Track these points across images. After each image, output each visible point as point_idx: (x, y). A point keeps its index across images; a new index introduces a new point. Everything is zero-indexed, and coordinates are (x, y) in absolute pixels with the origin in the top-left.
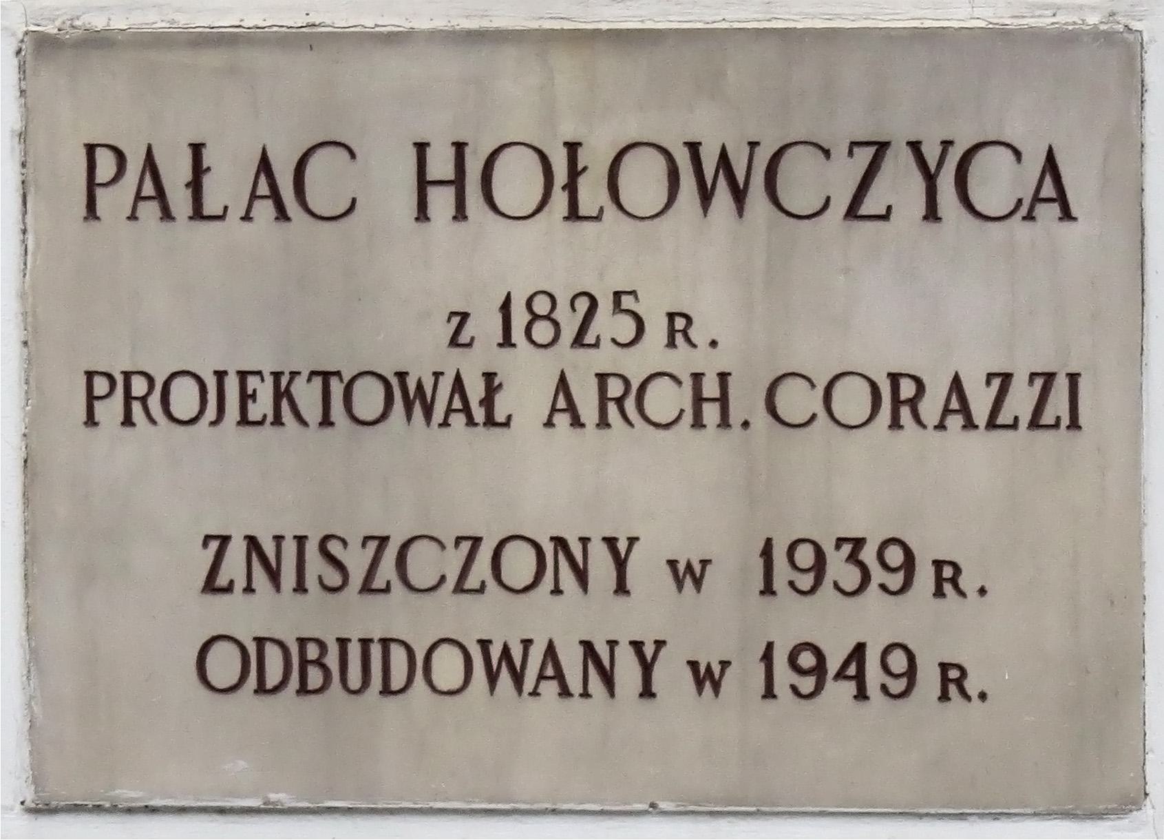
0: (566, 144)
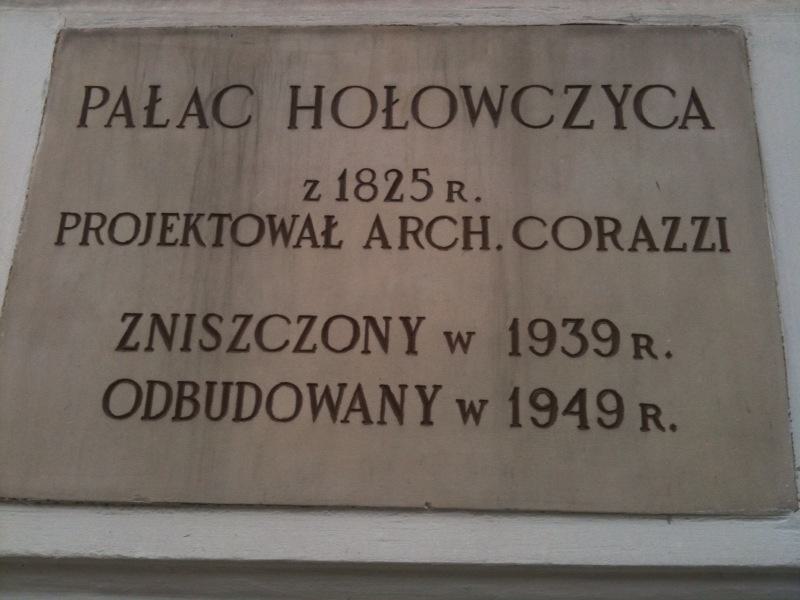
0: (386, 87)
